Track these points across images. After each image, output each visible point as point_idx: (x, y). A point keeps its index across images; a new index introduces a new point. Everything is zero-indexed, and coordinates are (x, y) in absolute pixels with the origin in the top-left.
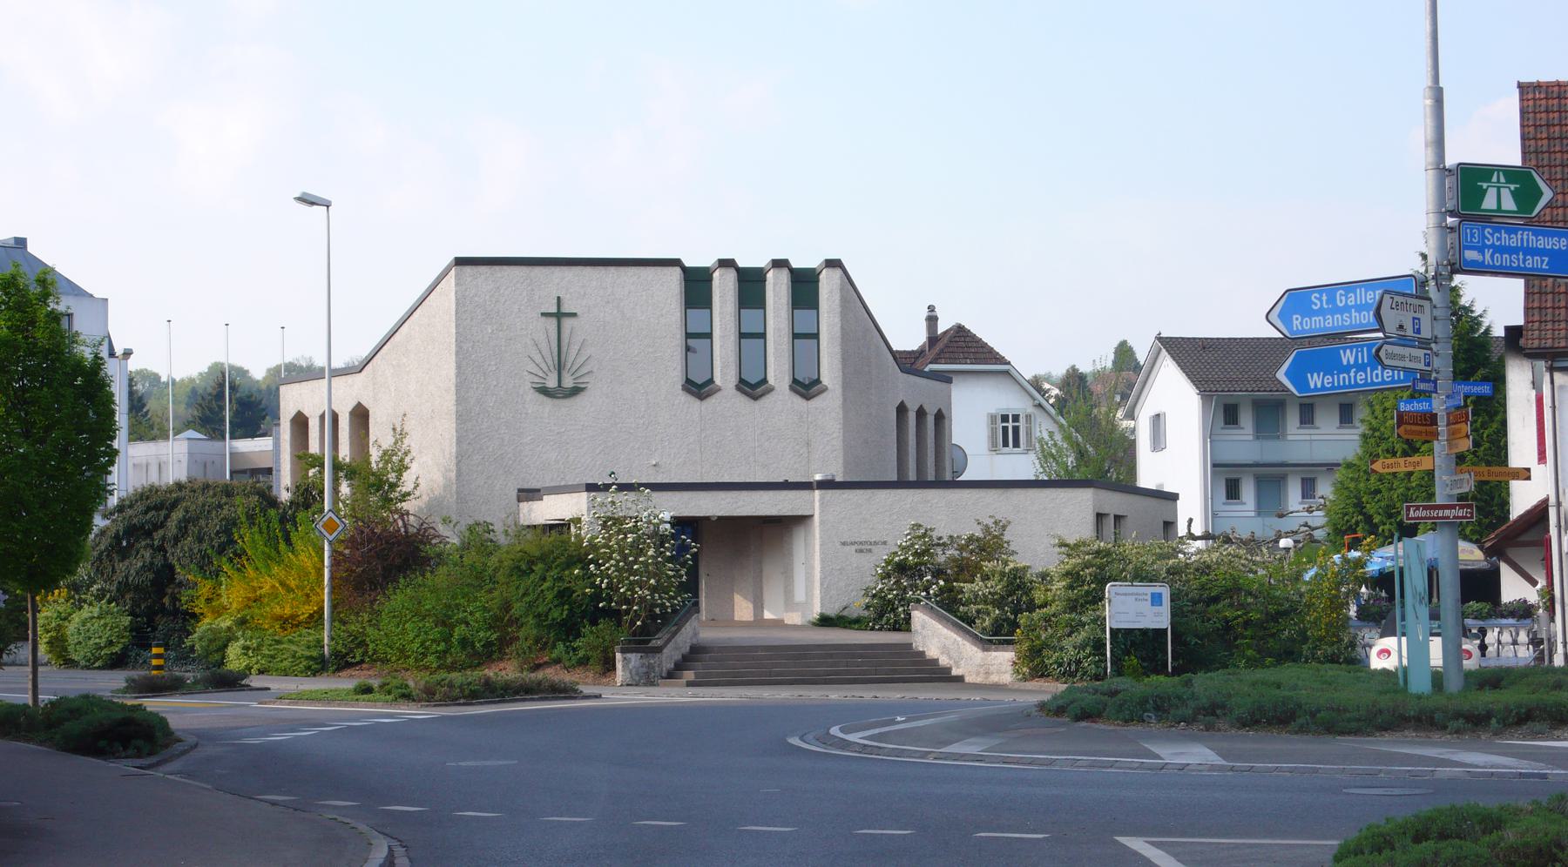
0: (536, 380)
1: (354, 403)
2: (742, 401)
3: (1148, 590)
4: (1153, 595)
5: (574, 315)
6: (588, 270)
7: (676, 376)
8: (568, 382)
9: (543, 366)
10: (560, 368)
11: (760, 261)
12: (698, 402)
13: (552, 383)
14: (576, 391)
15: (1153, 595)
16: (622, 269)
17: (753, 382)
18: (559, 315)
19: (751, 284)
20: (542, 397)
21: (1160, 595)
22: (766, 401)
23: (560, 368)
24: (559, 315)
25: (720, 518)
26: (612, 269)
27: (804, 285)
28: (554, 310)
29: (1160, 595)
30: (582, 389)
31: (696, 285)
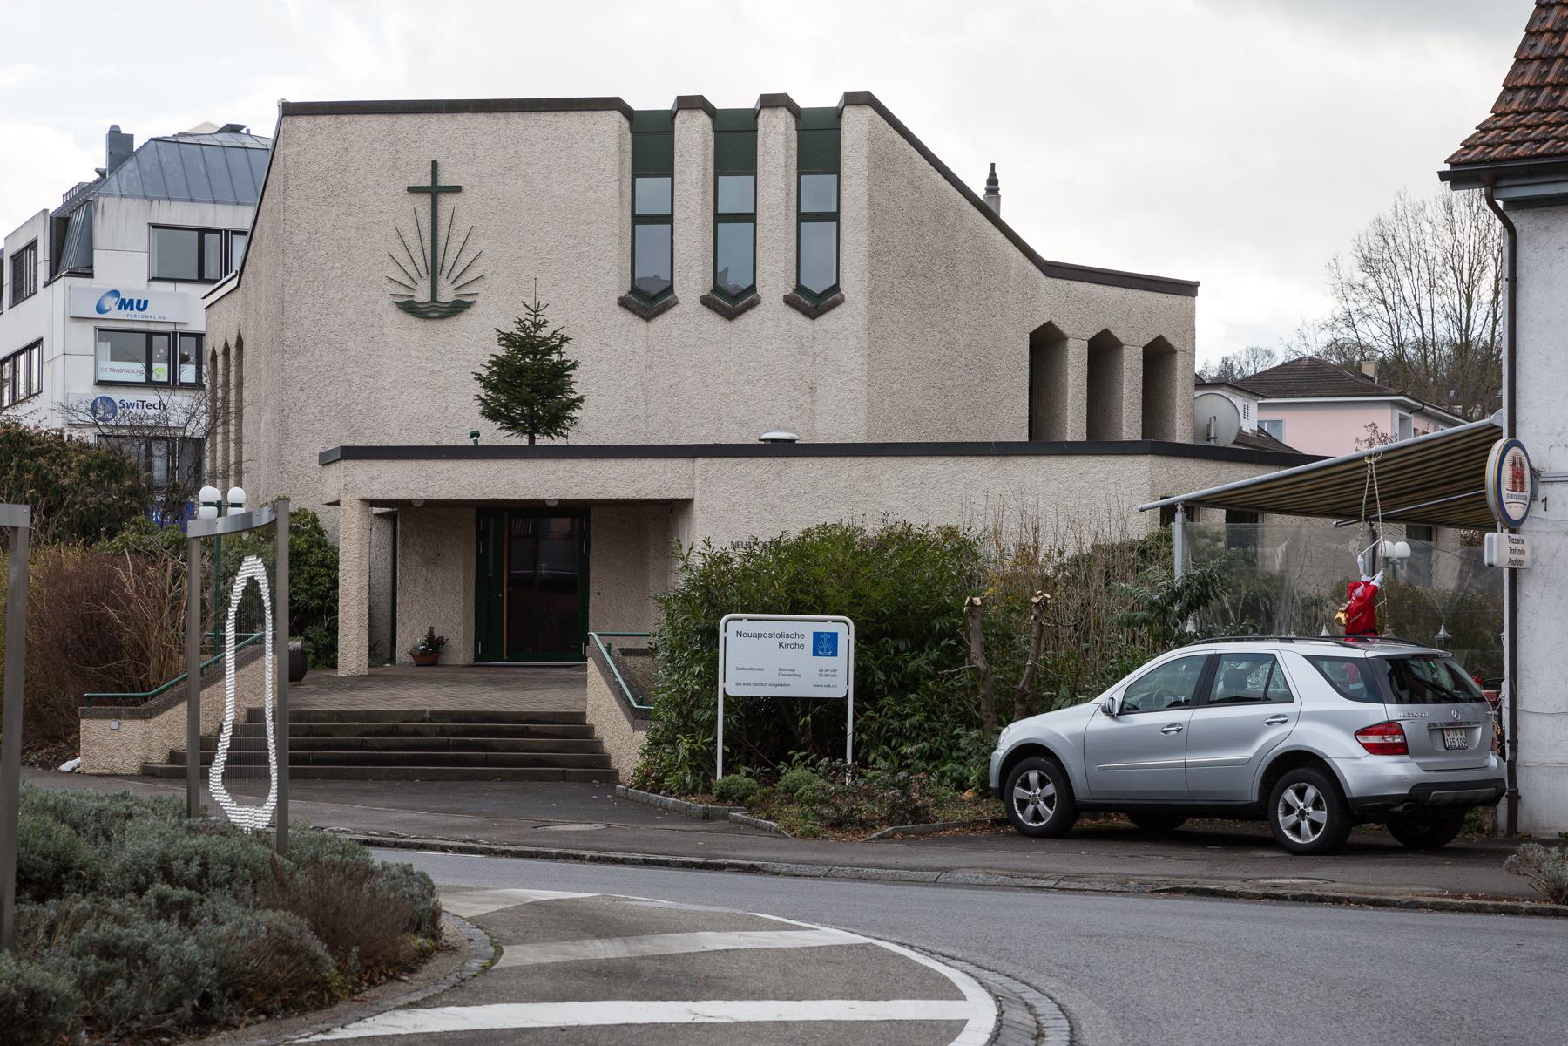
0: (402, 291)
1: (625, 317)
2: (711, 321)
3: (806, 627)
4: (817, 637)
5: (457, 189)
6: (481, 119)
7: (616, 283)
8: (447, 294)
9: (414, 274)
10: (434, 272)
11: (829, 98)
12: (644, 323)
13: (422, 295)
14: (458, 307)
15: (817, 637)
16: (532, 117)
17: (818, 290)
18: (435, 191)
19: (735, 138)
20: (410, 319)
21: (833, 637)
22: (750, 319)
23: (434, 272)
24: (435, 191)
25: (562, 502)
26: (517, 118)
27: (818, 138)
28: (427, 182)
29: (833, 637)
30: (469, 305)
31: (651, 140)
